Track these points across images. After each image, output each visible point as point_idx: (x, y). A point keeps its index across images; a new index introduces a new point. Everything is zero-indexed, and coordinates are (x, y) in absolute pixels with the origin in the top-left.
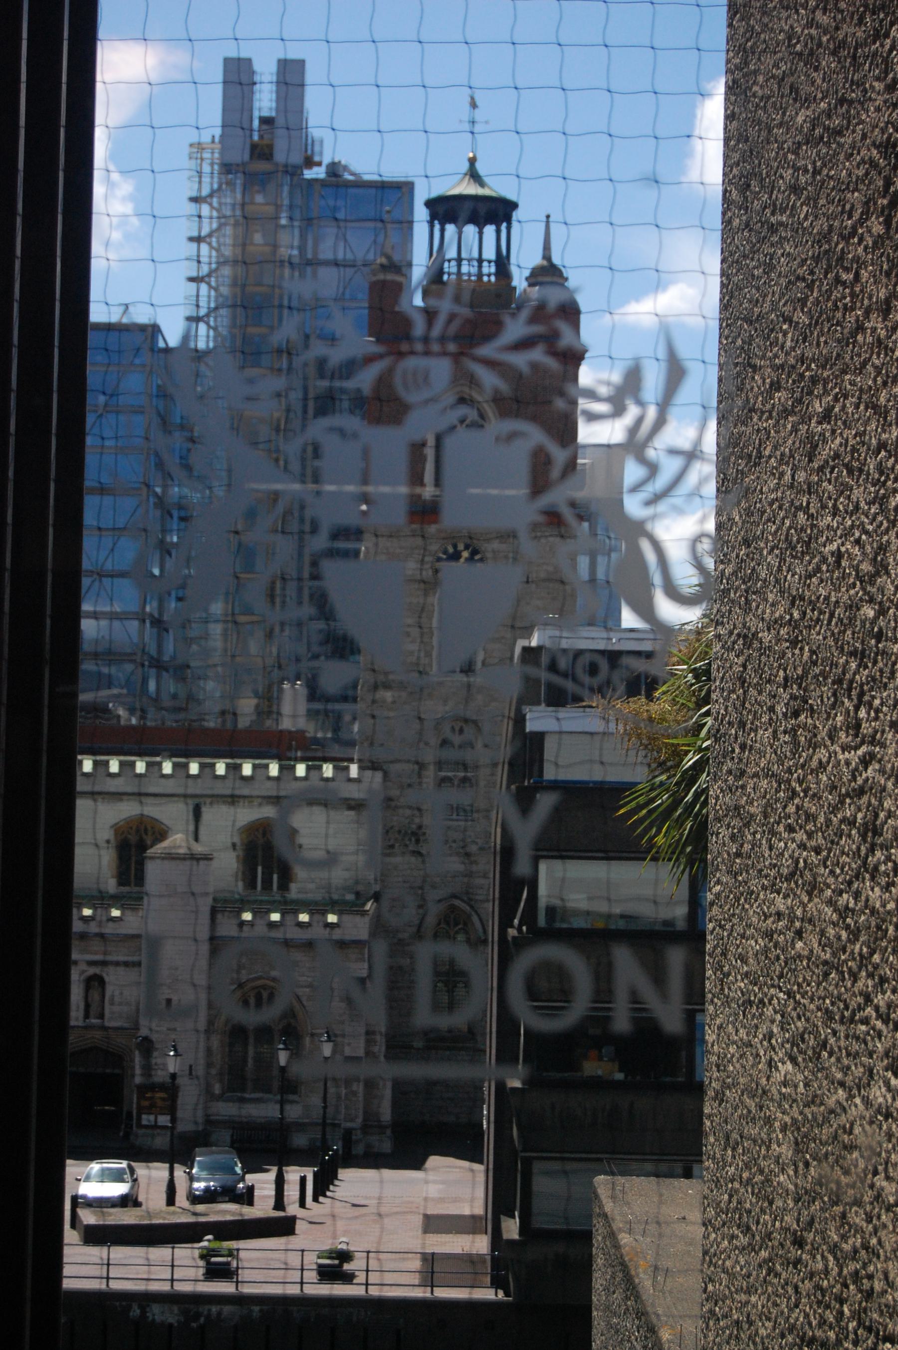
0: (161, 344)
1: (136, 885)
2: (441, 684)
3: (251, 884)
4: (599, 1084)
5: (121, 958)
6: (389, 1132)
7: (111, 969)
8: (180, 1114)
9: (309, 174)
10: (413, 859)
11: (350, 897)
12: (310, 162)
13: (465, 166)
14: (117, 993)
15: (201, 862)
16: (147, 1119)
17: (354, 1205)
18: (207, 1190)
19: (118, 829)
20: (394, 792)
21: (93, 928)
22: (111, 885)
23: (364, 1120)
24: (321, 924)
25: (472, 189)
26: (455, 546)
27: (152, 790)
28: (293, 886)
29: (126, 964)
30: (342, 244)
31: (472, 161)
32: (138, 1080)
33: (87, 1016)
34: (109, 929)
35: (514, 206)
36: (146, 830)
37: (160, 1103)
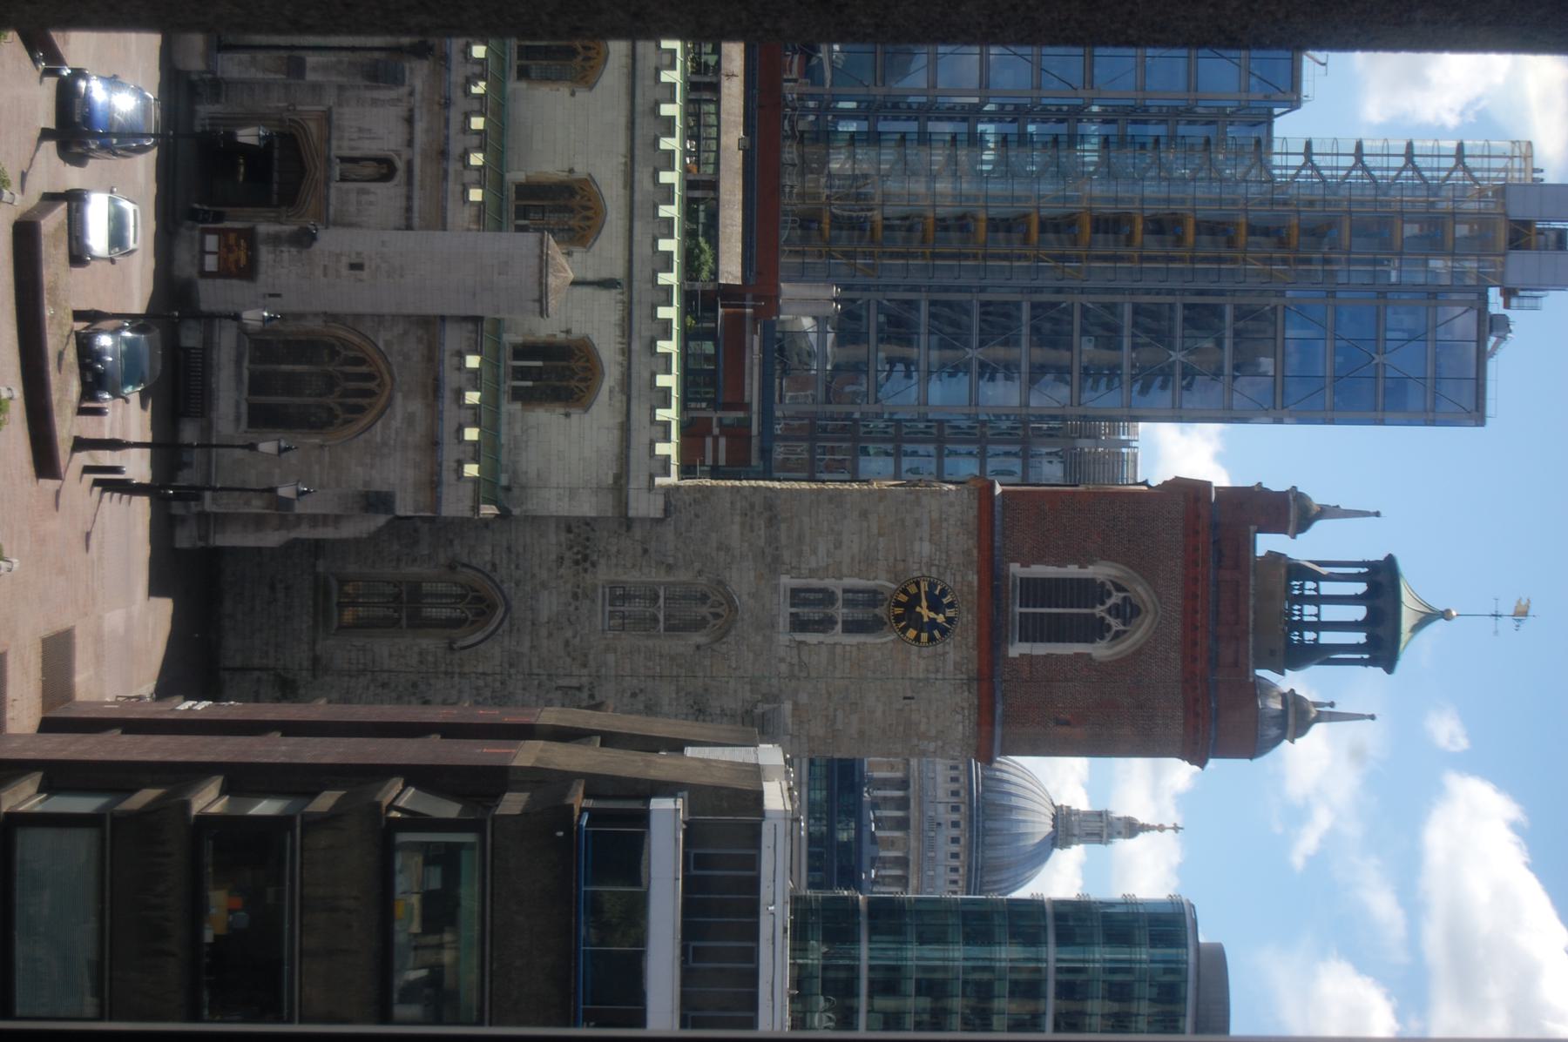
0: (1277, 111)
1: (517, 207)
2: (776, 588)
3: (522, 351)
4: (197, 910)
5: (416, 203)
6: (201, 544)
7: (403, 190)
8: (219, 282)
9: (1494, 295)
10: (553, 557)
11: (504, 480)
12: (1508, 294)
13: (1440, 606)
14: (372, 198)
15: (537, 305)
16: (212, 242)
17: (88, 535)
18: (98, 355)
20: (638, 533)
21: (454, 167)
22: (516, 176)
23: (216, 514)
24: (461, 456)
25: (1407, 620)
26: (951, 605)
27: (638, 225)
28: (518, 406)
30: (1405, 336)
31: (1446, 615)
32: (264, 228)
33: (343, 160)
34: (453, 187)
35: (1389, 668)
36: (588, 218)
37: (232, 257)
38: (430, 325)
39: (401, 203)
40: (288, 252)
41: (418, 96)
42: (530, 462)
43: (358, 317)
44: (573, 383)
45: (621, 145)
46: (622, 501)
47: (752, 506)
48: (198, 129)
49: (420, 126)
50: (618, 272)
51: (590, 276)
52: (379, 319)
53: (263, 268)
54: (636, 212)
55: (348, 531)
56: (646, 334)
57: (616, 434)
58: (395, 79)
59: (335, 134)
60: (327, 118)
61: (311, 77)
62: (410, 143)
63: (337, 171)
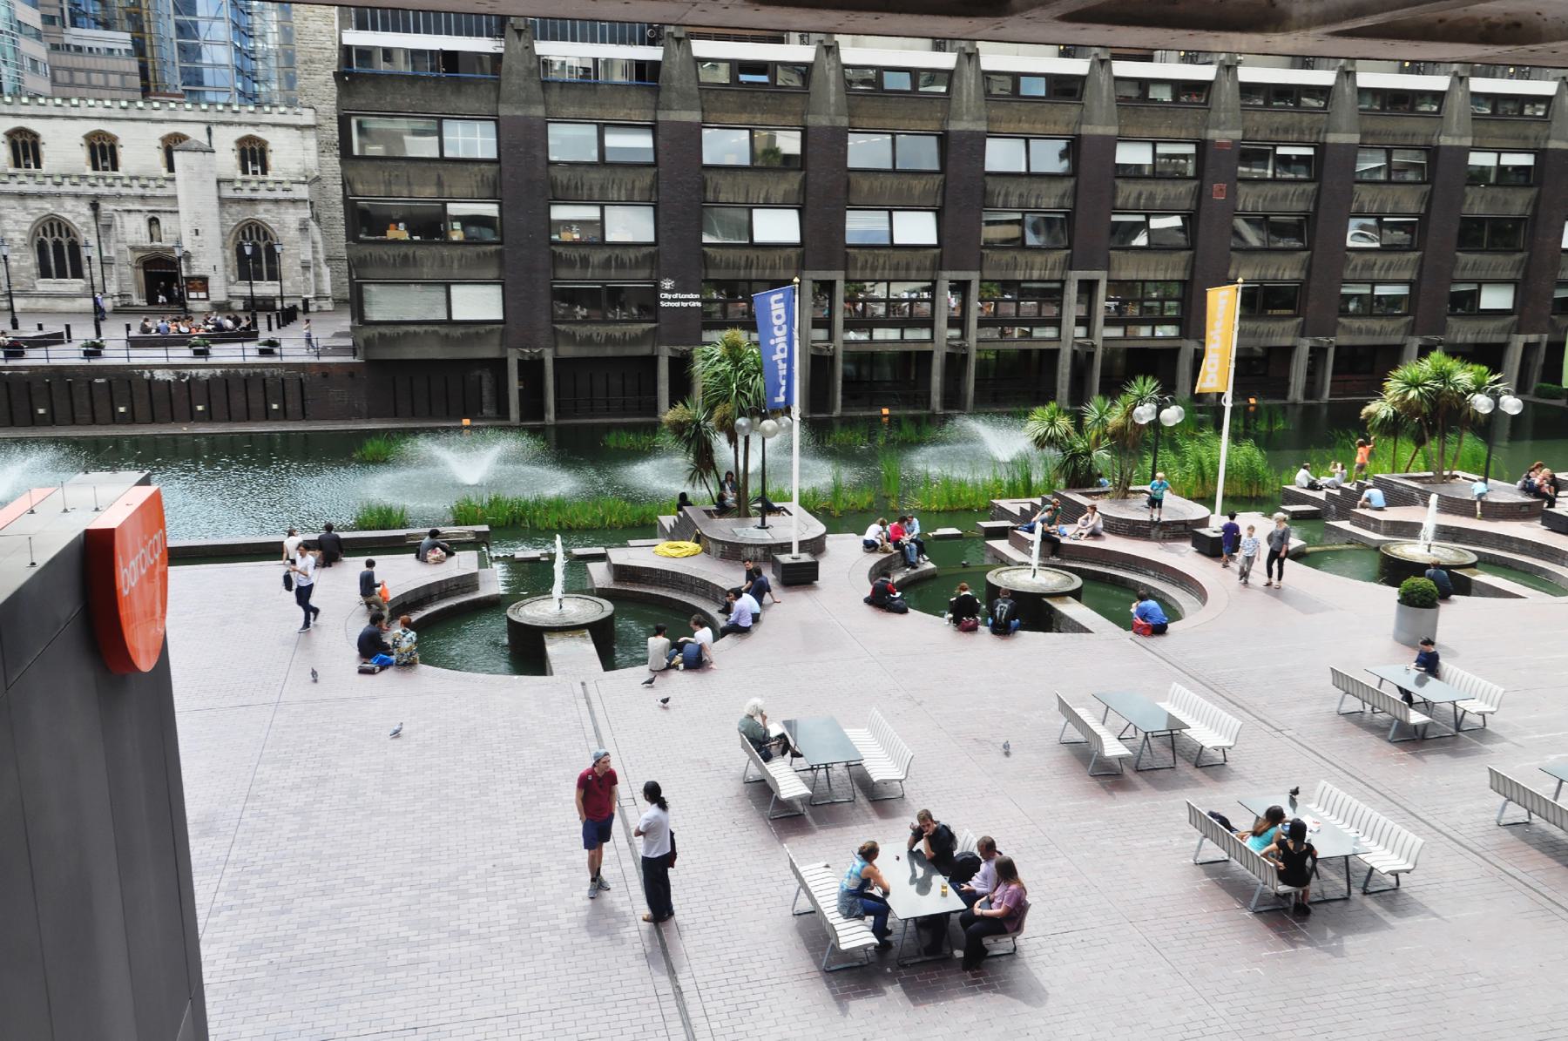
3: (245, 171)
16: (193, 295)
19: (163, 140)
20: (322, 121)
38: (222, 201)
40: (194, 262)
42: (294, 168)
49: (131, 207)
50: (204, 127)
52: (222, 224)
55: (318, 238)
58: (112, 217)
60: (133, 249)
61: (113, 254)
63: (157, 244)
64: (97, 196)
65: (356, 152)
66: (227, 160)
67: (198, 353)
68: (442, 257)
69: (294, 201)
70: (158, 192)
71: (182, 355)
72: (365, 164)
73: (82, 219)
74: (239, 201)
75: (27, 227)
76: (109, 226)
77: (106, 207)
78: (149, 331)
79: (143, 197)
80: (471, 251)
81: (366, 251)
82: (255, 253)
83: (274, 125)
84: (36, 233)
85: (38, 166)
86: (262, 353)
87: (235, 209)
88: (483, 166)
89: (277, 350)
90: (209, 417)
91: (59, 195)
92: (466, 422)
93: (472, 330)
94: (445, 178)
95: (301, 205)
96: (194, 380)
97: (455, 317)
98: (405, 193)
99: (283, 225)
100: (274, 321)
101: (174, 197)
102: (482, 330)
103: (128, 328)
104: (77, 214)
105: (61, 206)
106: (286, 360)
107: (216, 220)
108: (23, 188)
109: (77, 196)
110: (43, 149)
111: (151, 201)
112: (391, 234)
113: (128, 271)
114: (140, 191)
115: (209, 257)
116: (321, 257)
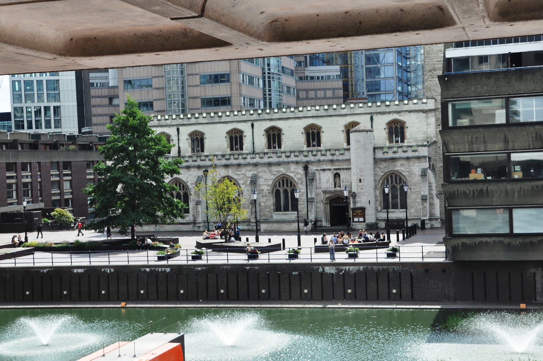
3: (391, 141)
5: (345, 167)
7: (342, 171)
8: (366, 217)
16: (356, 219)
27: (356, 112)
28: (405, 141)
29: (347, 169)
32: (352, 206)
33: (335, 187)
37: (359, 214)
38: (376, 161)
39: (345, 171)
40: (358, 199)
41: (318, 168)
42: (421, 137)
43: (375, 181)
44: (399, 126)
45: (336, 118)
46: (431, 111)
47: (431, 75)
48: (329, 225)
49: (325, 167)
50: (369, 117)
51: (370, 124)
53: (362, 206)
54: (353, 113)
55: (433, 180)
56: (384, 108)
57: (412, 114)
58: (314, 174)
59: (329, 189)
60: (325, 192)
61: (313, 196)
62: (330, 170)
63: (338, 189)
64: (308, 162)
65: (451, 124)
66: (381, 135)
67: (351, 256)
68: (507, 191)
69: (419, 158)
70: (341, 158)
71: (341, 257)
72: (456, 132)
73: (299, 176)
74: (385, 160)
75: (270, 183)
76: (312, 180)
77: (312, 168)
78: (326, 242)
79: (332, 161)
80: (527, 186)
81: (454, 188)
82: (394, 191)
83: (410, 111)
84: (275, 186)
85: (280, 147)
86: (389, 256)
87: (383, 165)
88: (537, 127)
89: (398, 254)
90: (354, 298)
91: (288, 163)
92: (523, 306)
93: (528, 240)
94: (509, 137)
95: (423, 160)
96: (347, 273)
97: (516, 231)
98: (482, 148)
99: (411, 174)
100: (401, 236)
101: (349, 160)
102: (535, 240)
103: (315, 240)
104: (296, 173)
105: (289, 169)
106: (402, 260)
107: (372, 172)
108: (270, 160)
109: (297, 163)
110: (283, 137)
111: (336, 164)
112: (472, 176)
113: (321, 206)
114: (330, 158)
115: (366, 195)
116: (434, 192)
